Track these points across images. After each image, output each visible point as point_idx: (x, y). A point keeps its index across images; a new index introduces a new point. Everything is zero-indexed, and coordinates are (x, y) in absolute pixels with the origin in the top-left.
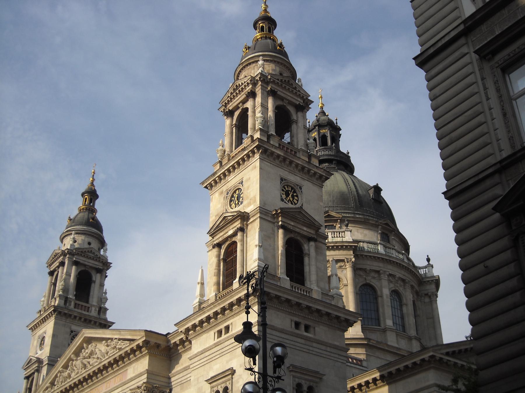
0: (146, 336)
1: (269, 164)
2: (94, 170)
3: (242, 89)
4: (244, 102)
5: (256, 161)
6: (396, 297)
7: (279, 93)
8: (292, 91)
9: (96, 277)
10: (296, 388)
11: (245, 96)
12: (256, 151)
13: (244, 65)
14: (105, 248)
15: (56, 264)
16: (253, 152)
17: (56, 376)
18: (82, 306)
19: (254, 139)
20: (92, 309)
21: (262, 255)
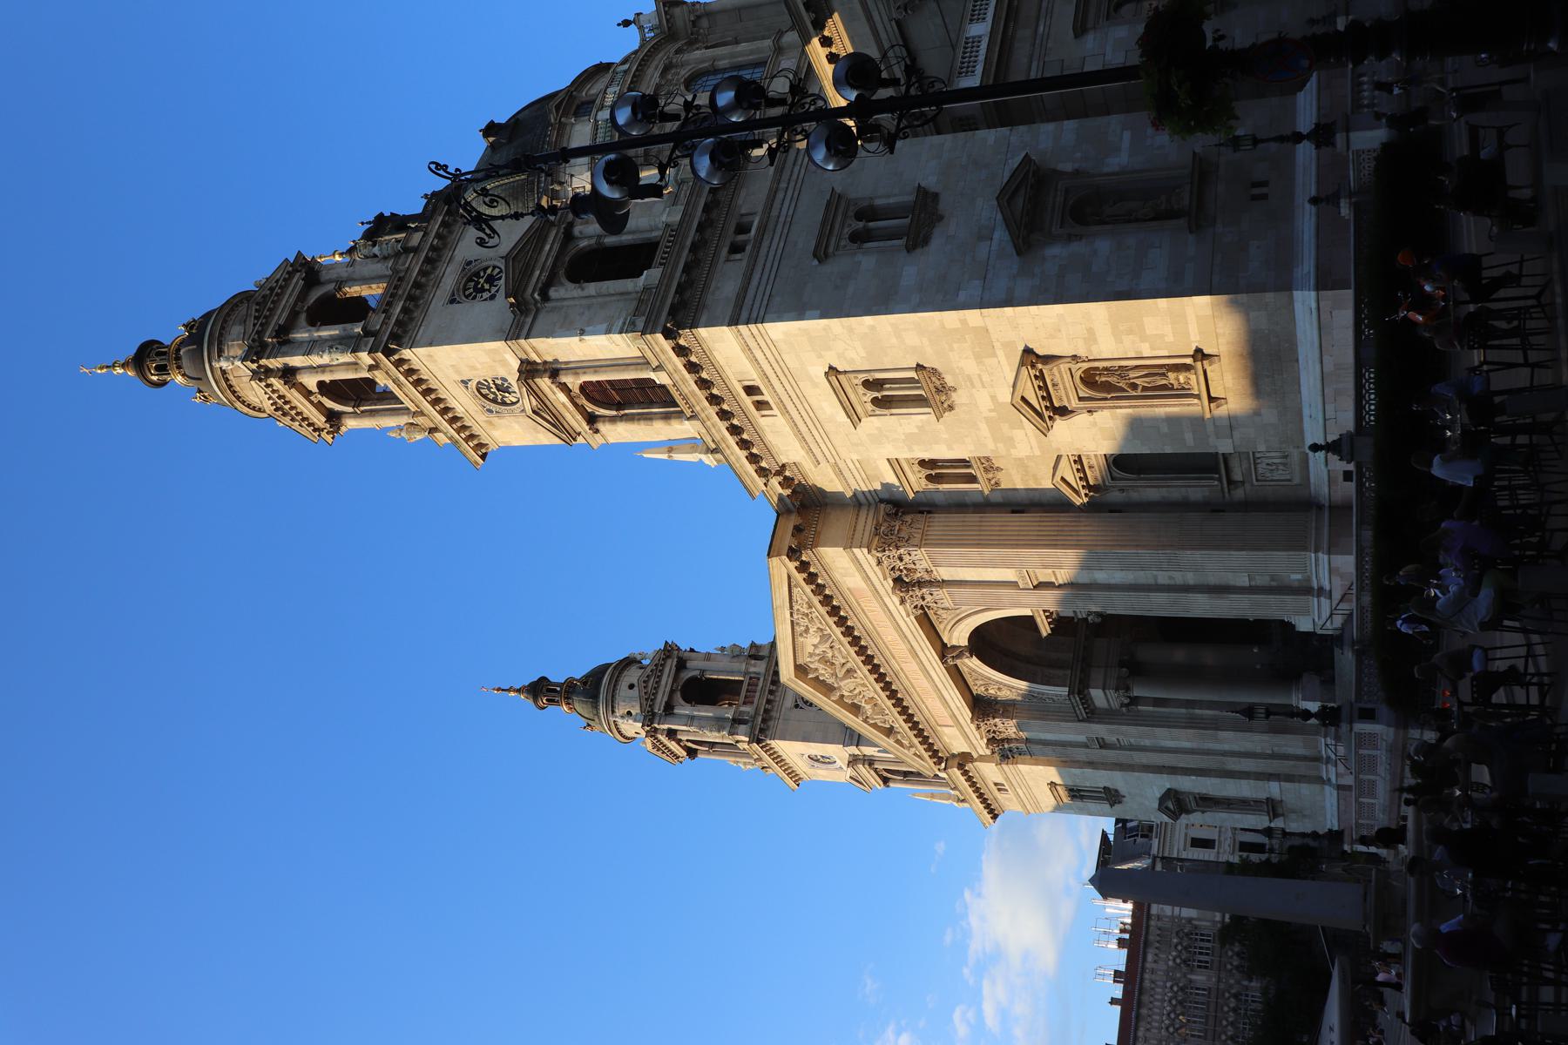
0: (779, 555)
1: (422, 328)
2: (494, 689)
3: (280, 397)
4: (307, 393)
5: (416, 356)
6: (700, 82)
7: (281, 322)
8: (277, 295)
9: (694, 668)
10: (859, 242)
11: (293, 390)
12: (396, 357)
13: (234, 399)
14: (639, 658)
15: (673, 745)
16: (399, 363)
17: (875, 726)
18: (748, 691)
19: (374, 363)
20: (755, 673)
21: (599, 327)
